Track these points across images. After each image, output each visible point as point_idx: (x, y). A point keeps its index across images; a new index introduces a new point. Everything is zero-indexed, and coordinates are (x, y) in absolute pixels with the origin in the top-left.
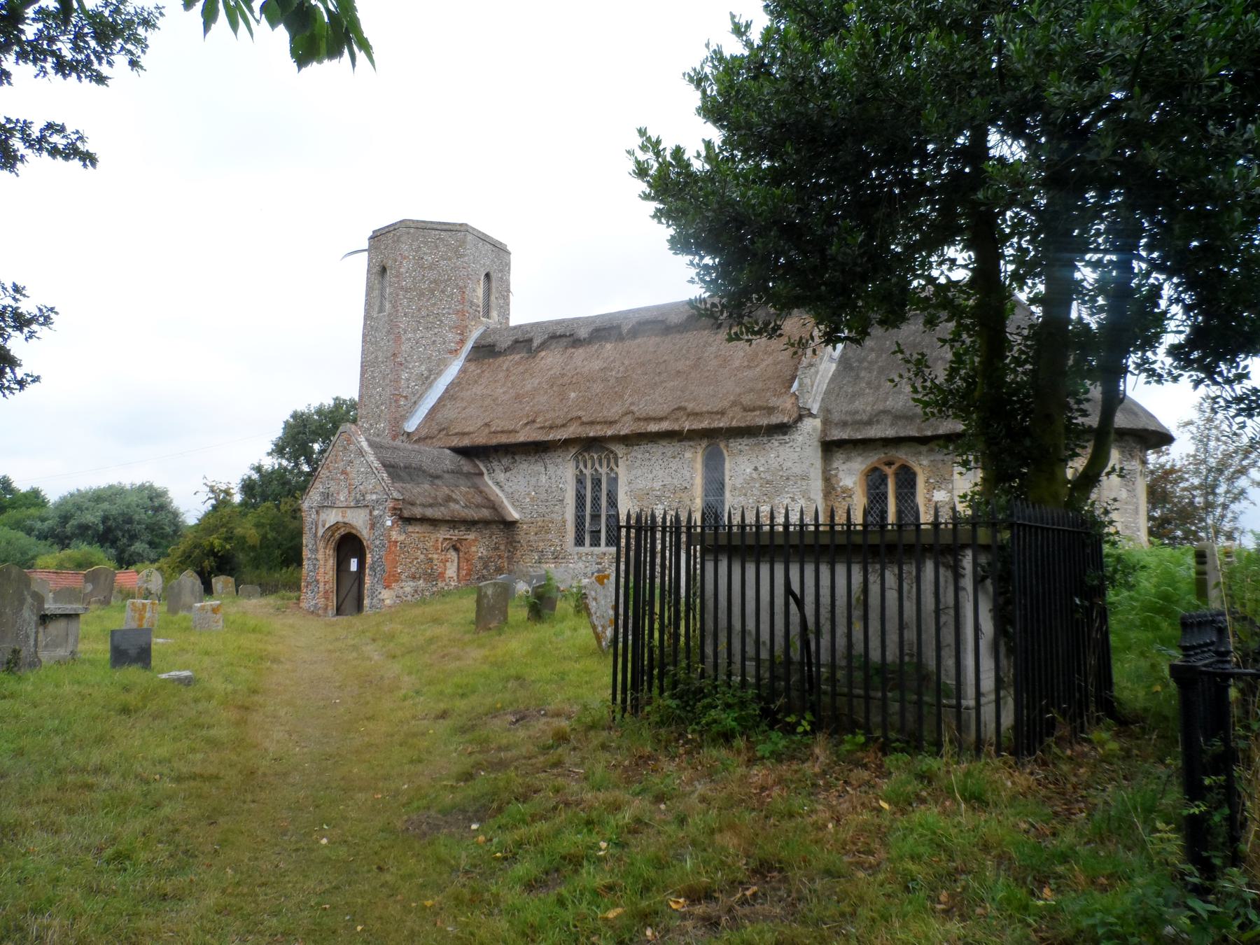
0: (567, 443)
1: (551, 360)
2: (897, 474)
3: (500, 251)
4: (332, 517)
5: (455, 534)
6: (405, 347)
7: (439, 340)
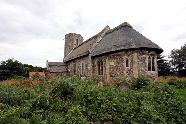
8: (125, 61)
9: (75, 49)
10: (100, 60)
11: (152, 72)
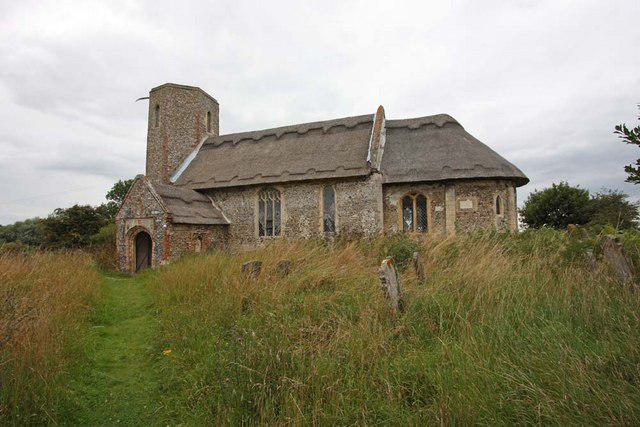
0: (253, 186)
1: (242, 149)
2: (417, 199)
3: (215, 103)
4: (133, 224)
5: (200, 231)
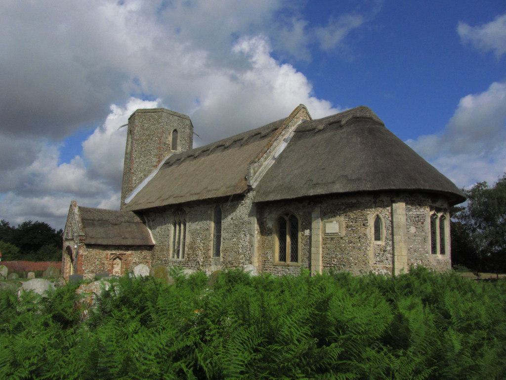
5: (118, 252)
6: (135, 166)
7: (149, 161)
8: (371, 222)
9: (168, 164)
10: (287, 215)
11: (439, 256)
